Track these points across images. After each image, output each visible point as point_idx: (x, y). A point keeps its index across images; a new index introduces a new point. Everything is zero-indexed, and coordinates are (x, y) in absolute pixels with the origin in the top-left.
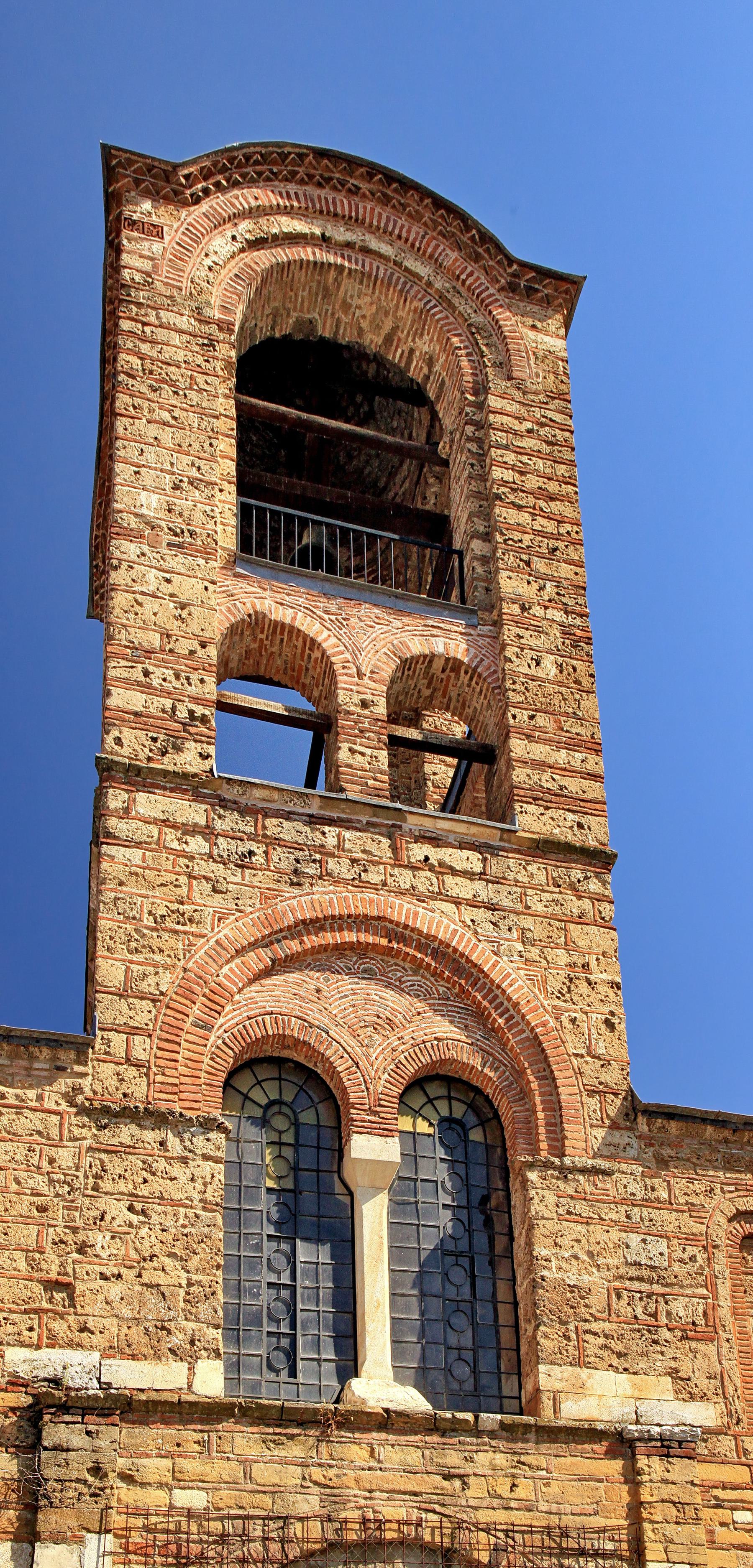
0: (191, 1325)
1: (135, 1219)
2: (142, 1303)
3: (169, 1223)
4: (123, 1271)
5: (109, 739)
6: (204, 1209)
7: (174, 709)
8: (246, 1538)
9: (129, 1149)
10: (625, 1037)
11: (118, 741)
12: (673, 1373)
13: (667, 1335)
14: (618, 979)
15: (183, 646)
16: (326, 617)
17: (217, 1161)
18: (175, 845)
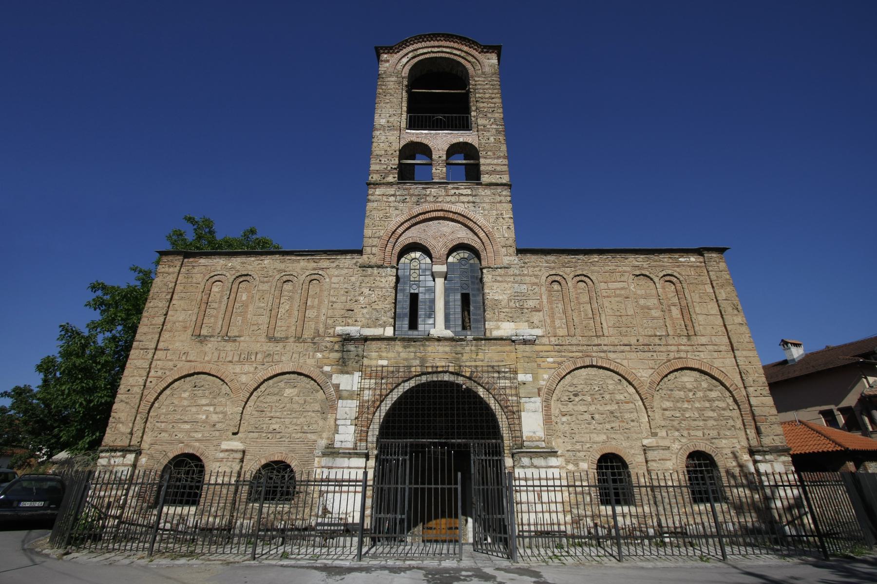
1: (370, 292)
2: (372, 313)
4: (367, 306)
5: (370, 177)
9: (370, 275)
10: (514, 231)
11: (372, 178)
13: (526, 311)
14: (512, 216)
15: (391, 152)
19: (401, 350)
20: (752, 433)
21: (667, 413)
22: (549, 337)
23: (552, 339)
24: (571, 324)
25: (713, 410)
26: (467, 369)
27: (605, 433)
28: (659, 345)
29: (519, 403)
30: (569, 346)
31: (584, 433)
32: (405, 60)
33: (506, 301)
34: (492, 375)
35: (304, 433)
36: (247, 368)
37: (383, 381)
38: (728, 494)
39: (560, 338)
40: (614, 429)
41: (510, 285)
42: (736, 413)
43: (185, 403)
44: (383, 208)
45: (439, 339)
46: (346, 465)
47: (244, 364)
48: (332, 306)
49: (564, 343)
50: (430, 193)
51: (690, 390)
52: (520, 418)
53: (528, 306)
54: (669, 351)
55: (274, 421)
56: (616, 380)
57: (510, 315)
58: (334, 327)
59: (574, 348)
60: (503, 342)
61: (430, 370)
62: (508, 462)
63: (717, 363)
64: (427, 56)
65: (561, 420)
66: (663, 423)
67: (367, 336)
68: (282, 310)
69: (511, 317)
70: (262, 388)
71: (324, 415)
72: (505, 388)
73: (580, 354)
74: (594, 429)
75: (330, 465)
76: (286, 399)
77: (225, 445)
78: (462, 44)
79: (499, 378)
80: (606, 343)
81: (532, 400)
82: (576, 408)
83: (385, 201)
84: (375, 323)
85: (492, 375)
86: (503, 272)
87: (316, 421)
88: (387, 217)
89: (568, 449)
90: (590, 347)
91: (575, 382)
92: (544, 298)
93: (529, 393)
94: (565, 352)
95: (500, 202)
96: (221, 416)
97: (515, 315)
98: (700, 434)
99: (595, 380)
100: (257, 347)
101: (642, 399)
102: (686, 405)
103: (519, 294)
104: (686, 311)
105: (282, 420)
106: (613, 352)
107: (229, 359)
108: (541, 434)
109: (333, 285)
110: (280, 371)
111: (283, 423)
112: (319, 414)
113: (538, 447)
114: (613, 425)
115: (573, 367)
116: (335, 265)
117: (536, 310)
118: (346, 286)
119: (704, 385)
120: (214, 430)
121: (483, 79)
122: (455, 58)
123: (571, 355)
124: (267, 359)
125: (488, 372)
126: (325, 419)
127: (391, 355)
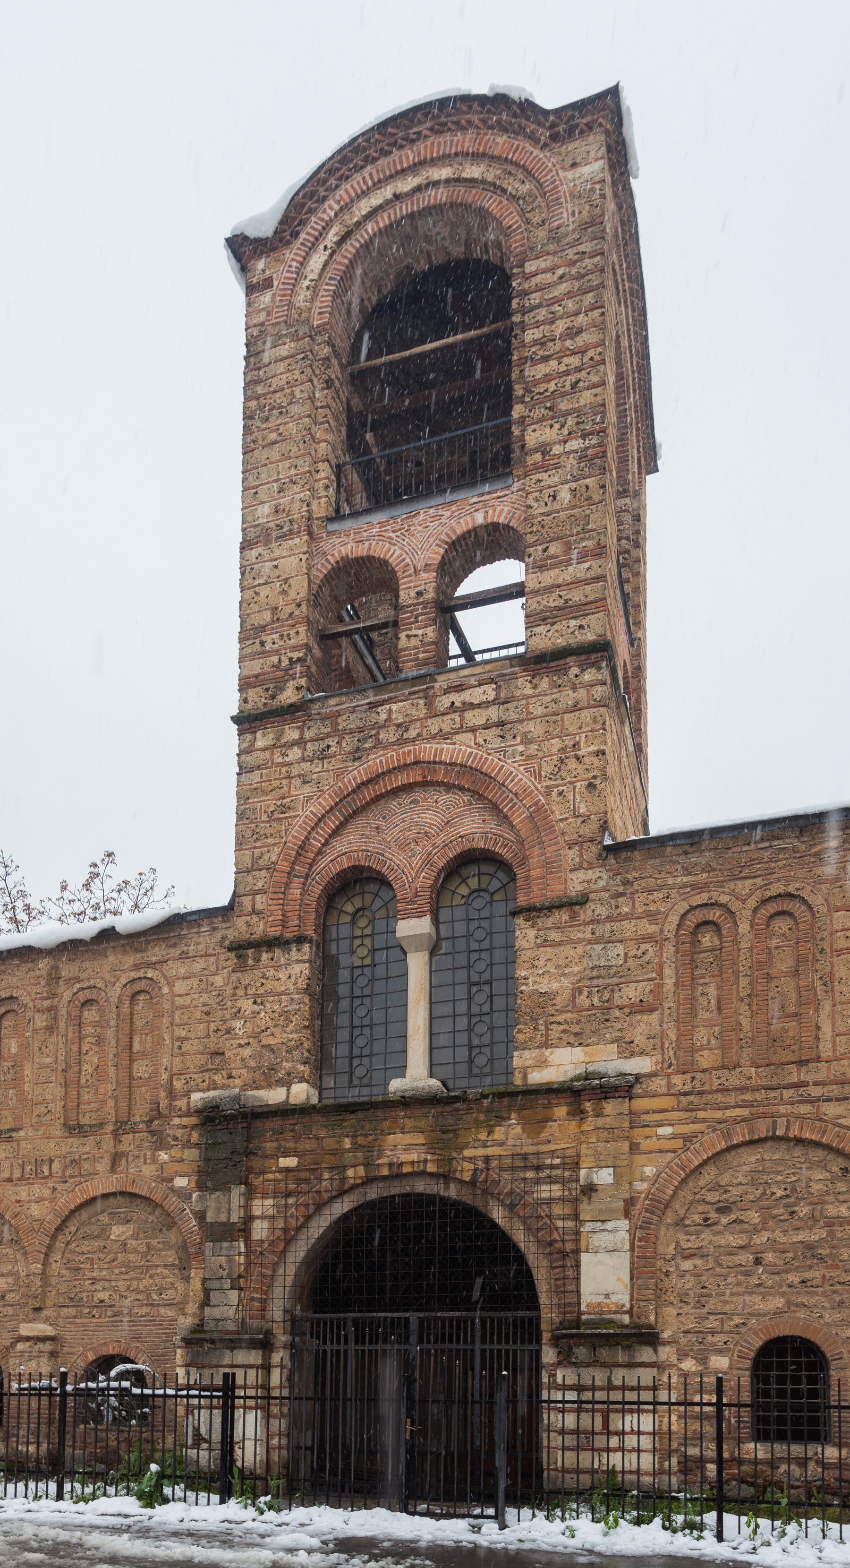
0: (287, 1065)
1: (256, 1008)
2: (261, 1056)
3: (276, 1007)
4: (251, 1040)
6: (298, 993)
7: (280, 661)
12: (617, 1040)
13: (617, 1013)
15: (288, 610)
16: (393, 535)
17: (304, 962)
18: (280, 760)
22: (669, 1075)
23: (677, 1080)
26: (467, 1166)
27: (783, 1294)
29: (577, 1233)
30: (719, 1095)
31: (732, 1294)
33: (567, 994)
34: (522, 1175)
35: (152, 1305)
36: (39, 1190)
37: (291, 1201)
39: (698, 1076)
40: (809, 1284)
41: (580, 950)
44: (275, 783)
47: (33, 1184)
48: (180, 1048)
49: (707, 1087)
50: (389, 719)
52: (577, 1266)
56: (835, 1169)
57: (575, 1029)
58: (187, 1094)
59: (732, 1099)
61: (385, 1172)
65: (677, 1267)
68: (87, 1068)
69: (576, 1034)
71: (185, 1272)
72: (550, 1201)
73: (745, 1112)
74: (759, 1285)
76: (115, 1246)
79: (538, 1181)
80: (819, 1077)
81: (610, 1225)
82: (721, 1240)
85: (522, 1175)
87: (172, 1284)
88: (284, 809)
89: (686, 1328)
90: (772, 1094)
91: (724, 1180)
92: (669, 971)
94: (705, 1110)
95: (576, 708)
97: (588, 1028)
99: (779, 1173)
100: (50, 1149)
103: (603, 972)
105: (113, 1284)
106: (838, 1100)
108: (623, 1298)
109: (179, 1001)
111: (115, 1289)
112: (176, 1271)
114: (807, 1275)
115: (723, 1145)
116: (178, 952)
117: (642, 1008)
118: (205, 998)
120: (5, 1306)
123: (719, 1115)
125: (513, 1169)
126: (187, 1279)
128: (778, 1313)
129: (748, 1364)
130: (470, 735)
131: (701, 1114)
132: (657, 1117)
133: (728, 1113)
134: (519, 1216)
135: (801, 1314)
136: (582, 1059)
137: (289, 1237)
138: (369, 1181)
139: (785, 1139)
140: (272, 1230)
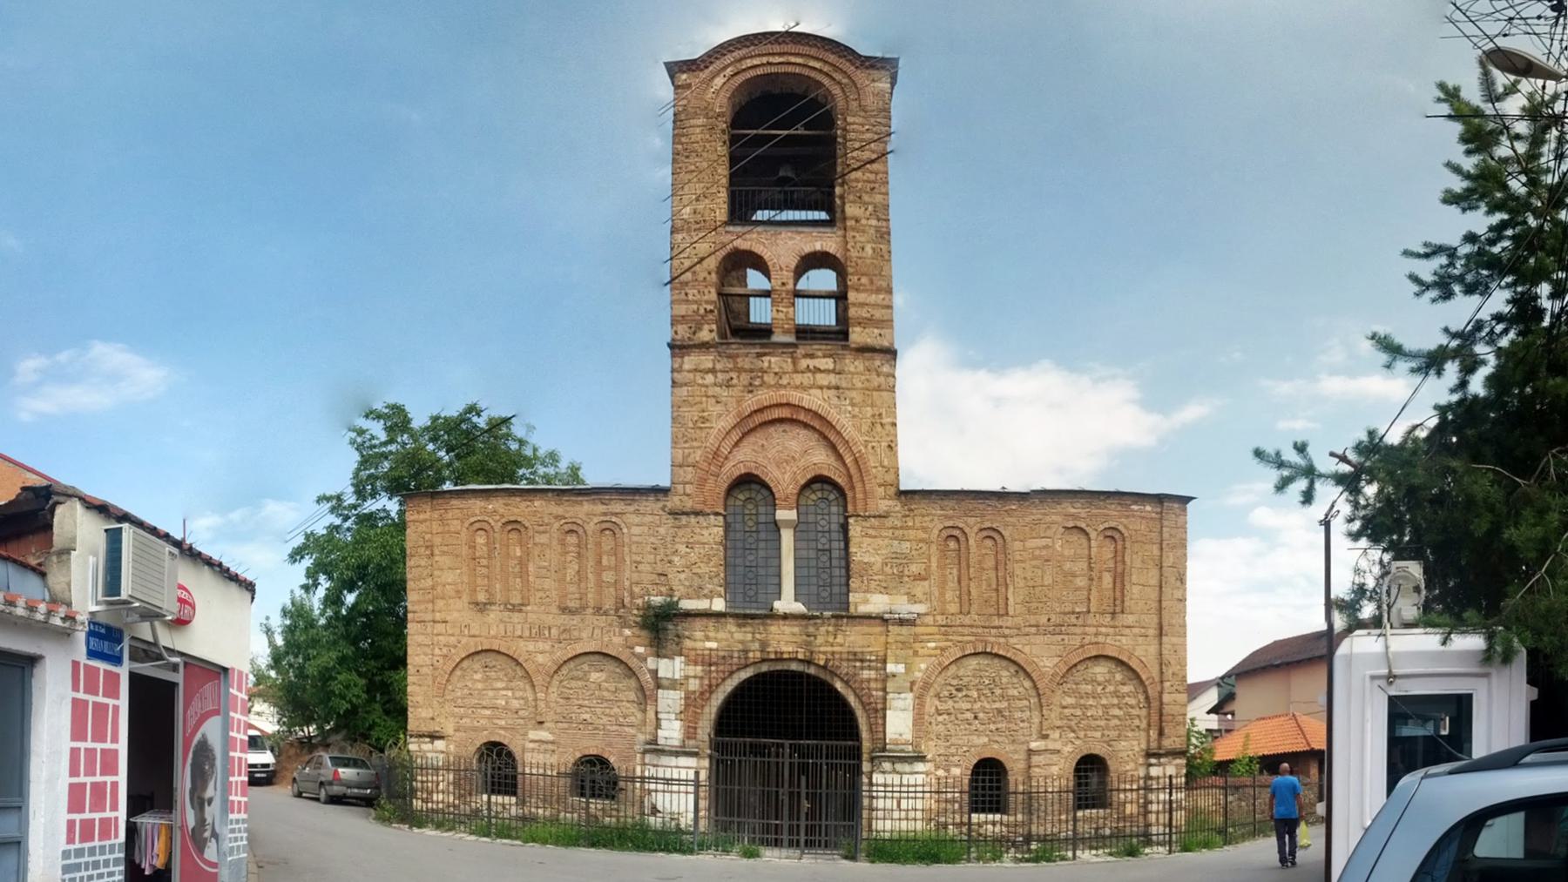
0: (710, 586)
8: (732, 657)
12: (908, 594)
13: (906, 579)
19: (734, 629)
20: (1153, 734)
21: (1066, 711)
23: (939, 618)
24: (965, 597)
25: (1120, 708)
26: (822, 656)
27: (987, 736)
28: (1075, 625)
29: (885, 699)
32: (719, 81)
36: (541, 645)
37: (713, 668)
38: (1115, 799)
42: (1144, 712)
43: (480, 686)
44: (698, 399)
45: (785, 617)
46: (673, 764)
51: (1099, 684)
52: (884, 717)
53: (911, 573)
54: (1086, 634)
55: (583, 710)
57: (885, 585)
59: (966, 631)
60: (872, 621)
61: (773, 656)
62: (866, 767)
63: (1139, 652)
64: (760, 71)
66: (1059, 723)
67: (689, 610)
70: (564, 671)
71: (642, 707)
72: (869, 680)
73: (972, 638)
75: (655, 763)
76: (594, 685)
77: (533, 735)
78: (826, 50)
79: (862, 668)
80: (1009, 624)
81: (903, 696)
82: (956, 706)
83: (699, 385)
84: (698, 593)
86: (877, 524)
88: (705, 420)
93: (900, 687)
96: (522, 702)
97: (891, 585)
98: (1098, 734)
100: (549, 620)
101: (1039, 695)
102: (1091, 702)
104: (1120, 579)
107: (519, 633)
108: (908, 736)
110: (582, 651)
111: (594, 713)
113: (902, 751)
114: (999, 726)
117: (919, 578)
119: (1118, 677)
121: (860, 120)
122: (813, 74)
123: (960, 638)
124: (564, 636)
125: (848, 660)
126: (644, 711)
127: (721, 635)
128: (984, 745)
129: (969, 772)
130: (819, 391)
131: (951, 637)
132: (926, 637)
133: (966, 638)
134: (851, 687)
135: (996, 746)
136: (888, 601)
137: (711, 689)
138: (763, 660)
139: (990, 654)
140: (701, 685)
